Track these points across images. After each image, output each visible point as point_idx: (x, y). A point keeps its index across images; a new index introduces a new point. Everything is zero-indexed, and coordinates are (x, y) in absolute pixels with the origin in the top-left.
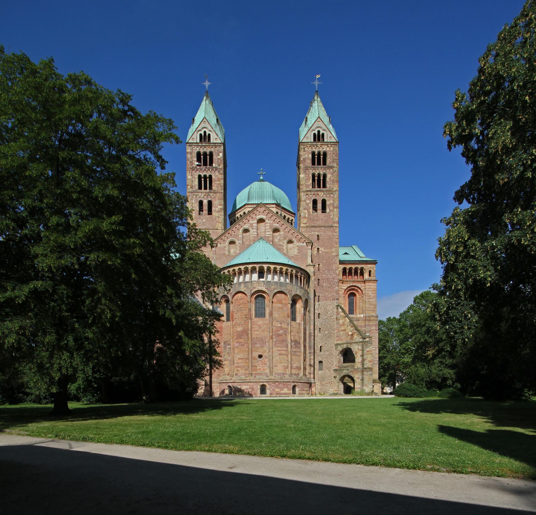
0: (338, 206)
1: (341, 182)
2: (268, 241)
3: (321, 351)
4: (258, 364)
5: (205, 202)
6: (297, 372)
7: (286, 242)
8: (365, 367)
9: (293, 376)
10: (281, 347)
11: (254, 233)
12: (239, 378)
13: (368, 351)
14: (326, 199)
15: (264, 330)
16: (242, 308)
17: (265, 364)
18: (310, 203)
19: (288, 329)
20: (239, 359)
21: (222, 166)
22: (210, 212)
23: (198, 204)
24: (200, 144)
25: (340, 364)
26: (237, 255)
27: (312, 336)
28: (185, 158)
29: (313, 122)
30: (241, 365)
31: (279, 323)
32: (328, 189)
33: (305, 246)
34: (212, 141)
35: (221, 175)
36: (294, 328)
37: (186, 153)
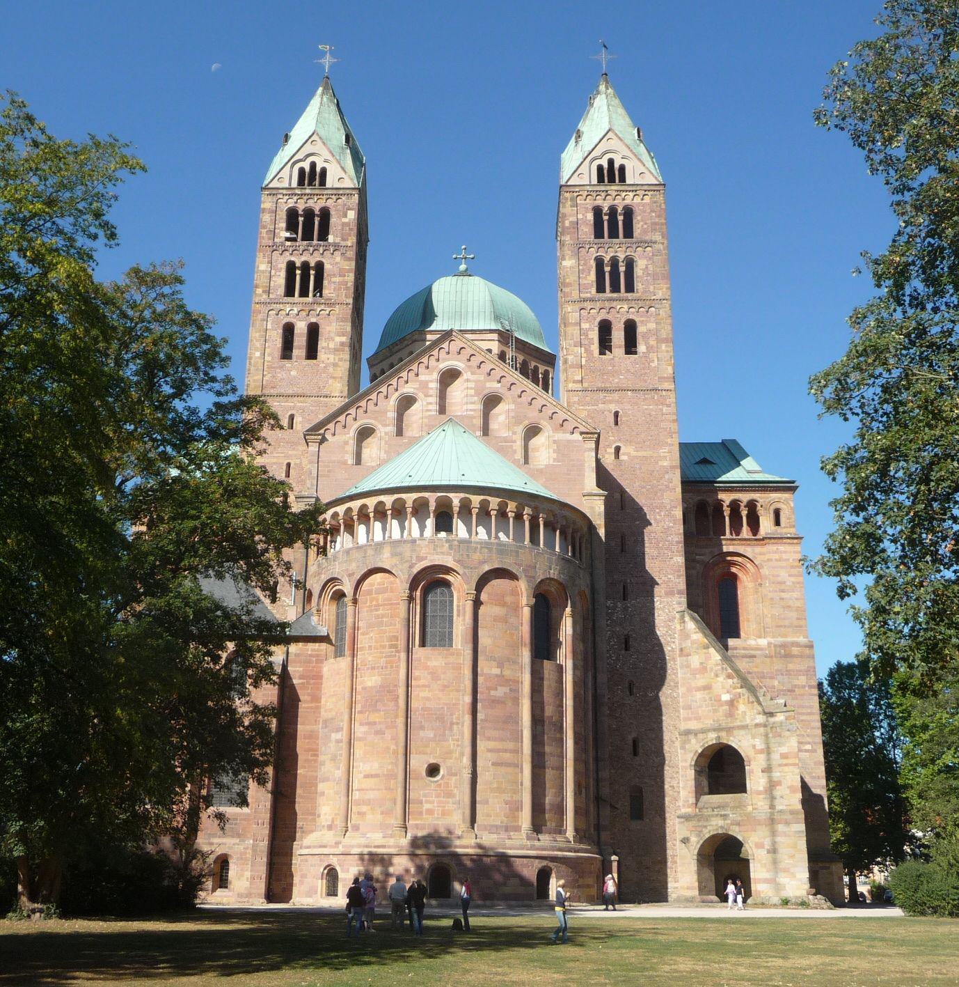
0: (671, 336)
1: (675, 274)
7: (520, 430)
10: (501, 740)
11: (430, 407)
12: (363, 841)
13: (784, 756)
14: (637, 320)
17: (449, 795)
20: (367, 776)
21: (352, 241)
24: (298, 192)
28: (256, 223)
30: (371, 795)
33: (575, 441)
34: (329, 184)
35: (346, 262)
37: (258, 211)
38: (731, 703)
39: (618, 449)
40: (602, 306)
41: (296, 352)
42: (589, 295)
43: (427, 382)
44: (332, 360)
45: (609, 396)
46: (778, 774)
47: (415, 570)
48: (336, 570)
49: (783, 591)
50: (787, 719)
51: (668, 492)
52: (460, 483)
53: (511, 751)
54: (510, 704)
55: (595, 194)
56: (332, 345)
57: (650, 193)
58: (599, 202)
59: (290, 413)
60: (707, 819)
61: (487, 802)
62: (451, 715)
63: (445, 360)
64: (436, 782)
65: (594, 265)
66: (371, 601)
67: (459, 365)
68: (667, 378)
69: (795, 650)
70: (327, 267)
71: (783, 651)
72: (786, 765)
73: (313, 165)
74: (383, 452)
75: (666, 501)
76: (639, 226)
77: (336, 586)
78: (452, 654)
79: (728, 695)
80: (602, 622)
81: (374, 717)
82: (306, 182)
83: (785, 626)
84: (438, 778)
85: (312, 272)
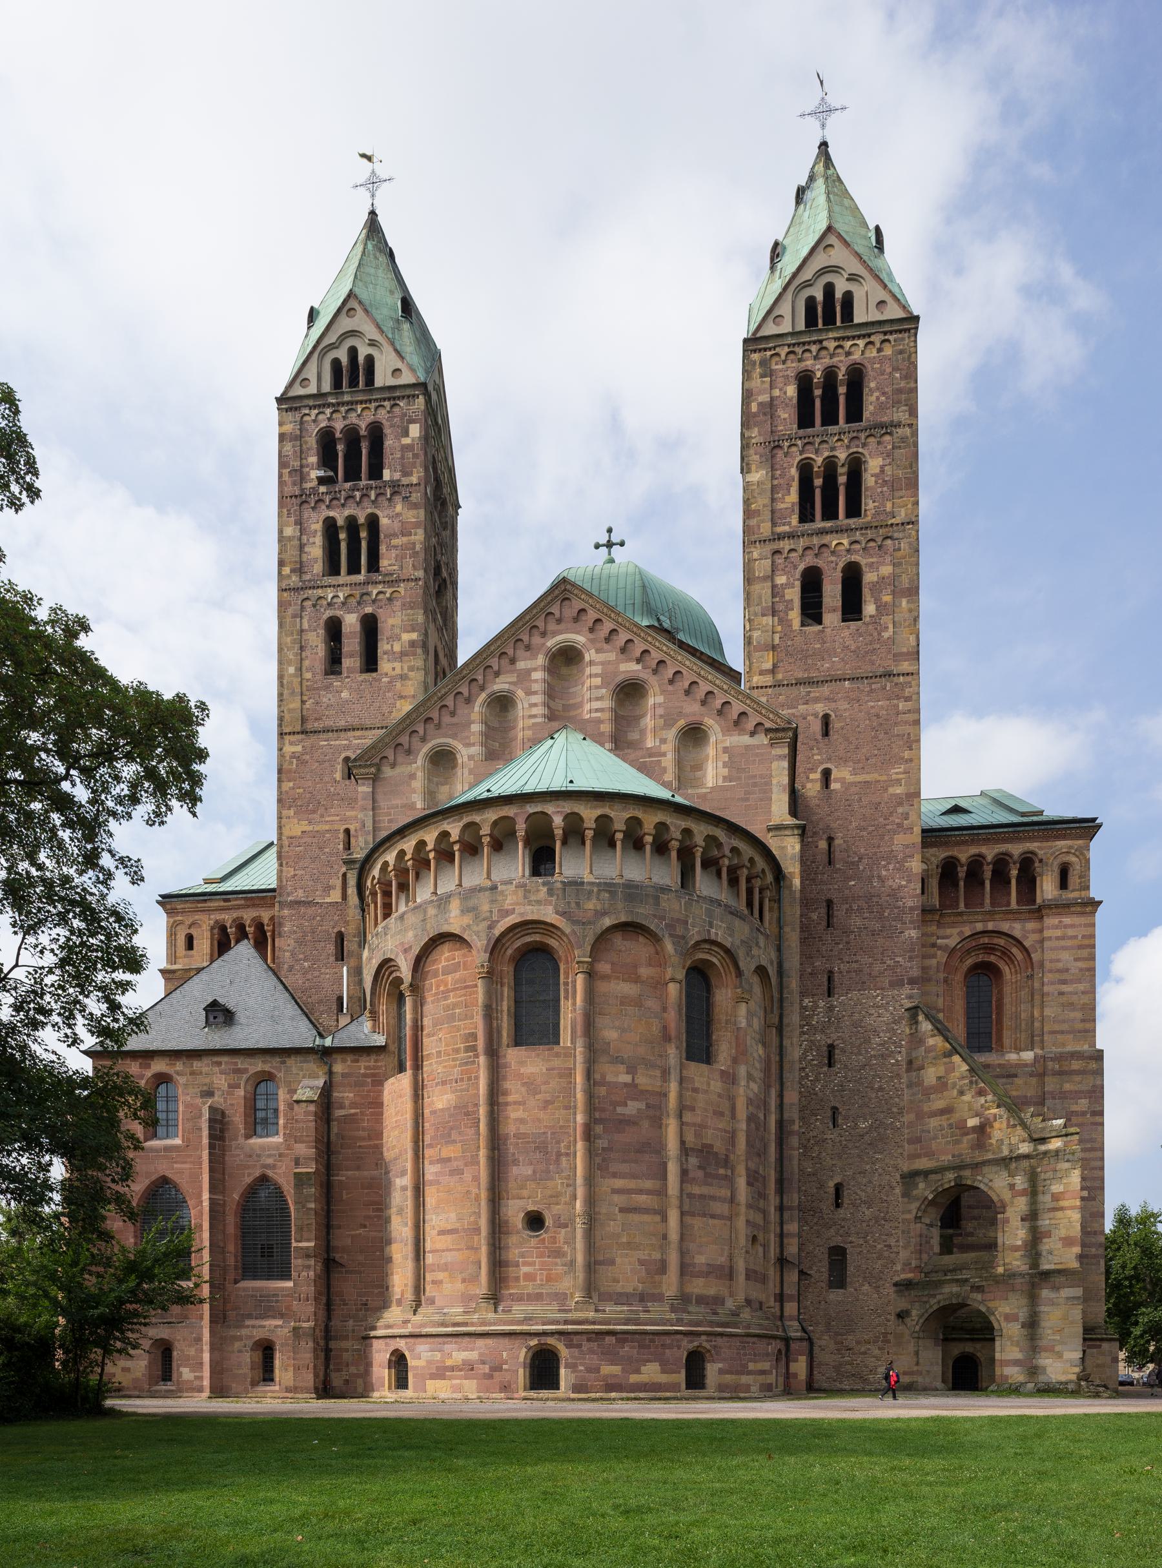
4: (523, 1256)
5: (351, 621)
6: (712, 1292)
8: (1045, 1266)
9: (691, 1309)
12: (436, 1318)
16: (455, 1006)
17: (558, 1253)
18: (789, 585)
19: (665, 1095)
20: (442, 1233)
25: (925, 1257)
27: (791, 1133)
30: (449, 1257)
34: (379, 382)
54: (646, 1124)
60: (939, 1284)
61: (612, 1262)
62: (558, 1142)
68: (908, 653)
78: (557, 1055)
80: (793, 1018)
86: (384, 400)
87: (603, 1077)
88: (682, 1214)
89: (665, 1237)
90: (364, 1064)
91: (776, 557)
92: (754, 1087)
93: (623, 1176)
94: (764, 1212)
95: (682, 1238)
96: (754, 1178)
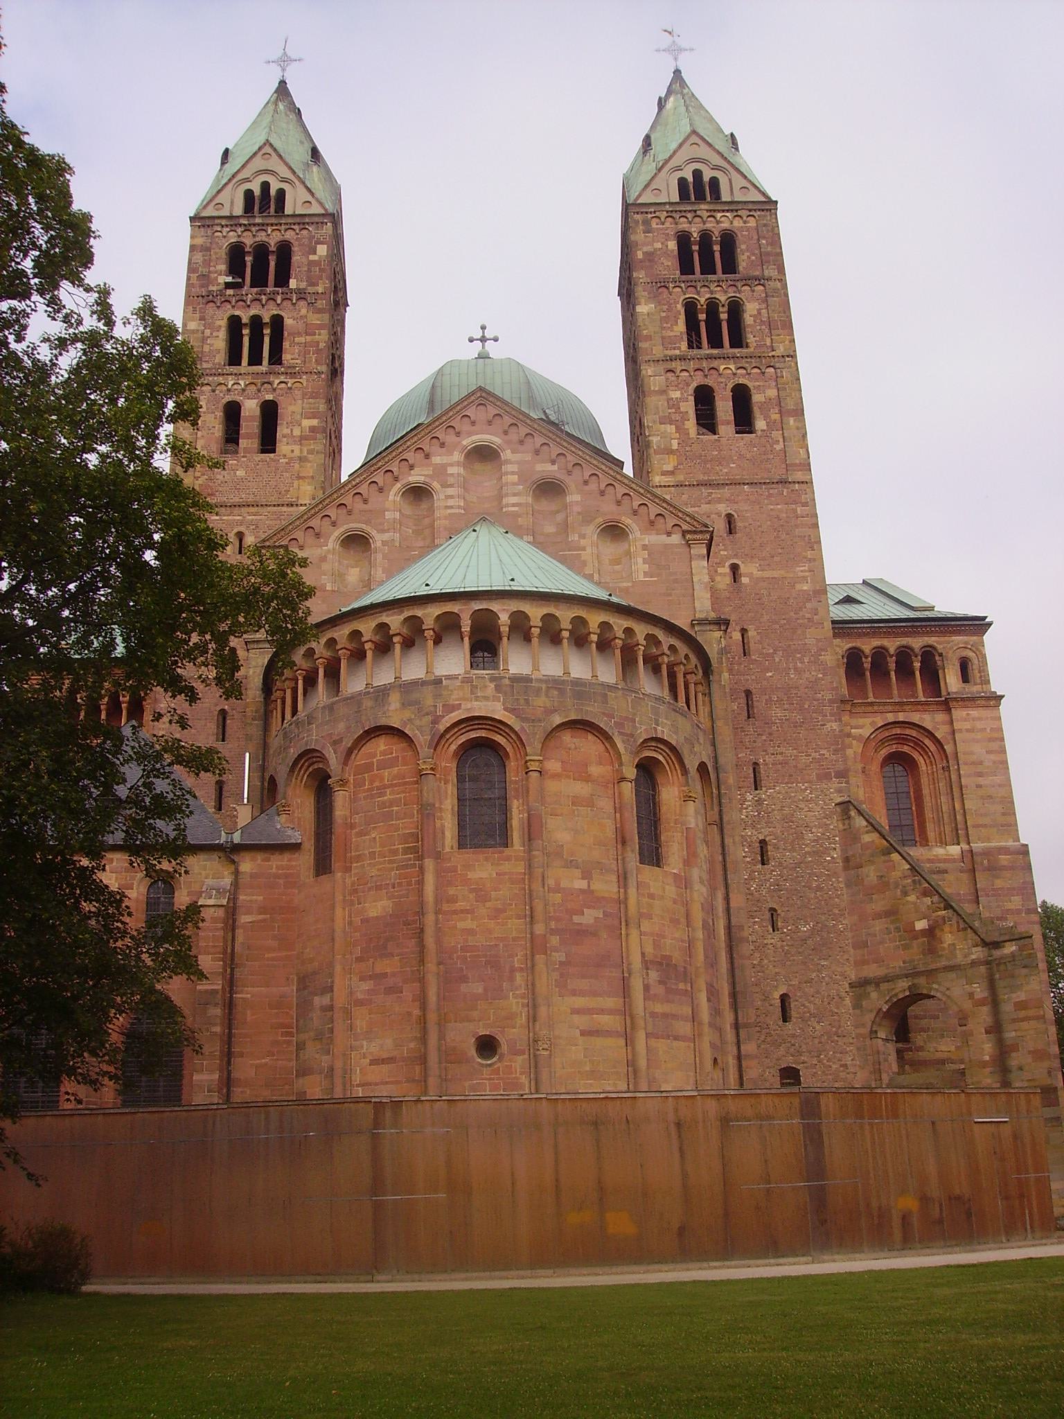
2: (513, 527)
3: (785, 1020)
7: (591, 531)
10: (595, 994)
11: (450, 502)
14: (750, 385)
15: (504, 911)
20: (374, 1062)
22: (268, 443)
23: (220, 414)
26: (368, 586)
29: (674, 146)
31: (578, 873)
32: (752, 350)
34: (288, 210)
35: (320, 315)
36: (651, 896)
38: (930, 932)
39: (735, 568)
40: (697, 367)
41: (243, 443)
42: (677, 352)
43: (444, 467)
44: (297, 453)
45: (717, 493)
46: (1014, 1034)
47: (442, 728)
48: (314, 737)
49: (980, 775)
50: (1021, 949)
51: (813, 628)
52: (508, 588)
53: (611, 1012)
55: (677, 216)
56: (297, 432)
57: (756, 214)
58: (684, 225)
59: (236, 530)
62: (511, 956)
63: (470, 434)
64: (490, 1065)
65: (683, 311)
66: (371, 782)
67: (495, 440)
69: (1004, 859)
70: (288, 322)
71: (985, 862)
72: (1023, 1020)
73: (265, 186)
74: (380, 570)
75: (810, 641)
76: (745, 257)
77: (313, 763)
78: (508, 859)
79: (926, 921)
80: (731, 816)
81: (384, 966)
82: (256, 208)
83: (985, 826)
84: (495, 1059)
85: (267, 331)
86: (294, 224)
87: (557, 883)
88: (647, 1035)
89: (632, 1063)
90: (277, 862)
91: (669, 374)
92: (704, 890)
93: (582, 993)
94: (720, 1030)
95: (648, 1067)
96: (712, 993)
